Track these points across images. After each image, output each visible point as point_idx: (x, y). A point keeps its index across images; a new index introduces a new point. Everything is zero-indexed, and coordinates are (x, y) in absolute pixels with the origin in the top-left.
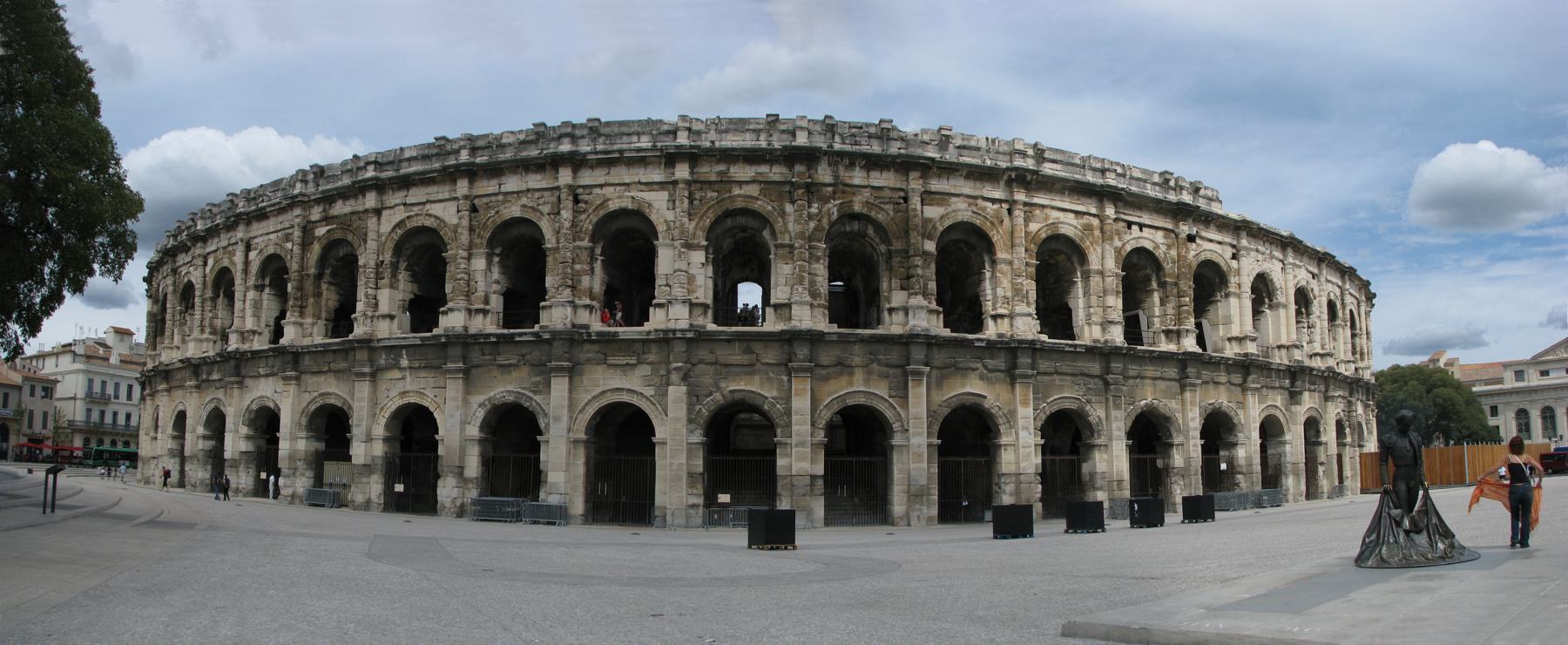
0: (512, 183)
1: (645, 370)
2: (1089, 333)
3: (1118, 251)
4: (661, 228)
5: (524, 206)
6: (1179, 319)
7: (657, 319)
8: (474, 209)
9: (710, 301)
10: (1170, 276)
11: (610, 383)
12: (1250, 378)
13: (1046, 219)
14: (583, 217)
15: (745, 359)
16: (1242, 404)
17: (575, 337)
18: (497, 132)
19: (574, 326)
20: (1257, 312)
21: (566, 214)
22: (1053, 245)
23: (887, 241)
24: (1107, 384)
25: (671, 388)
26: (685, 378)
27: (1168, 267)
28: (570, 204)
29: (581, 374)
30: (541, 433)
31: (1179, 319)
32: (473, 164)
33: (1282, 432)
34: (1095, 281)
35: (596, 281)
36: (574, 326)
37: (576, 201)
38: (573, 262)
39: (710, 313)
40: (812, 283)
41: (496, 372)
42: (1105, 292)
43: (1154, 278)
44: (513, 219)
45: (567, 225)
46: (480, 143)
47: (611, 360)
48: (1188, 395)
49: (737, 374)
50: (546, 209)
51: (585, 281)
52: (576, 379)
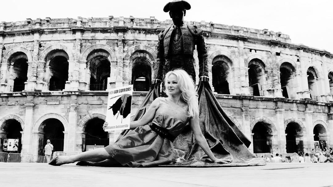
0: (18, 39)
1: (62, 106)
2: (234, 91)
3: (246, 60)
4: (70, 56)
5: (21, 48)
6: (273, 86)
7: (68, 87)
8: (4, 48)
9: (88, 82)
10: (269, 69)
11: (48, 110)
12: (307, 109)
13: (216, 49)
14: (43, 51)
15: (99, 102)
16: (304, 119)
17: (37, 94)
18: (14, 21)
19: (35, 90)
20: (310, 83)
21: (36, 50)
22: (220, 59)
23: (153, 60)
24: (242, 111)
25: (70, 113)
26: (76, 109)
27: (268, 65)
28: (38, 47)
29: (38, 108)
30: (22, 130)
31: (273, 86)
32: (5, 32)
33: (325, 132)
34: (236, 71)
35: (48, 74)
36: (35, 90)
37: (40, 46)
38: (37, 67)
39: (88, 87)
40: (124, 75)
41: (7, 107)
42: (241, 76)
43: (263, 69)
44: (18, 52)
45: (36, 54)
46: (8, 25)
47: (48, 103)
48: (278, 115)
49: (95, 108)
50: (29, 49)
51: (41, 75)
52: (36, 110)
